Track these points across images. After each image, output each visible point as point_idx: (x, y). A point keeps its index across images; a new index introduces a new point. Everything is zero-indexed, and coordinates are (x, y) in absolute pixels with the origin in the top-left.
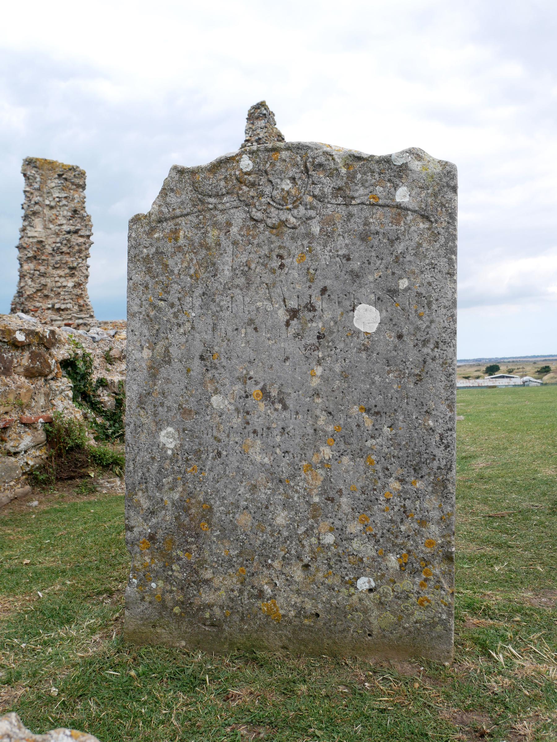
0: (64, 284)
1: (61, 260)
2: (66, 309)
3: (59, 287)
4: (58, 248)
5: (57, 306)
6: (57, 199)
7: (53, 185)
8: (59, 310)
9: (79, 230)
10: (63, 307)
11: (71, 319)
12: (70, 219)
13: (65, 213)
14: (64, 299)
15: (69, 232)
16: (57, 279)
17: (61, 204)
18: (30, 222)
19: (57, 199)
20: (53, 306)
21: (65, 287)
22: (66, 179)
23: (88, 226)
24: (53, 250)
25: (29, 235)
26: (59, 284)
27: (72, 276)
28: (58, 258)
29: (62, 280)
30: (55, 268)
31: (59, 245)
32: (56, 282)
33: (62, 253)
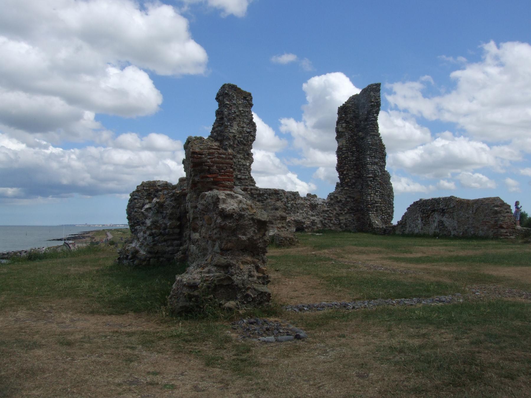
0: (244, 163)
1: (243, 149)
2: (245, 179)
3: (240, 165)
4: (241, 141)
5: (239, 176)
6: (242, 112)
7: (240, 102)
8: (240, 179)
9: (251, 131)
10: (243, 177)
11: (247, 186)
12: (247, 125)
13: (245, 120)
14: (244, 173)
15: (248, 132)
16: (240, 160)
17: (243, 115)
18: (231, 124)
19: (242, 112)
20: (237, 176)
21: (244, 165)
22: (247, 100)
23: (255, 130)
24: (239, 142)
25: (231, 131)
26: (241, 163)
27: (248, 159)
28: (242, 147)
29: (243, 161)
30: (238, 153)
31: (242, 139)
32: (239, 161)
33: (245, 145)
